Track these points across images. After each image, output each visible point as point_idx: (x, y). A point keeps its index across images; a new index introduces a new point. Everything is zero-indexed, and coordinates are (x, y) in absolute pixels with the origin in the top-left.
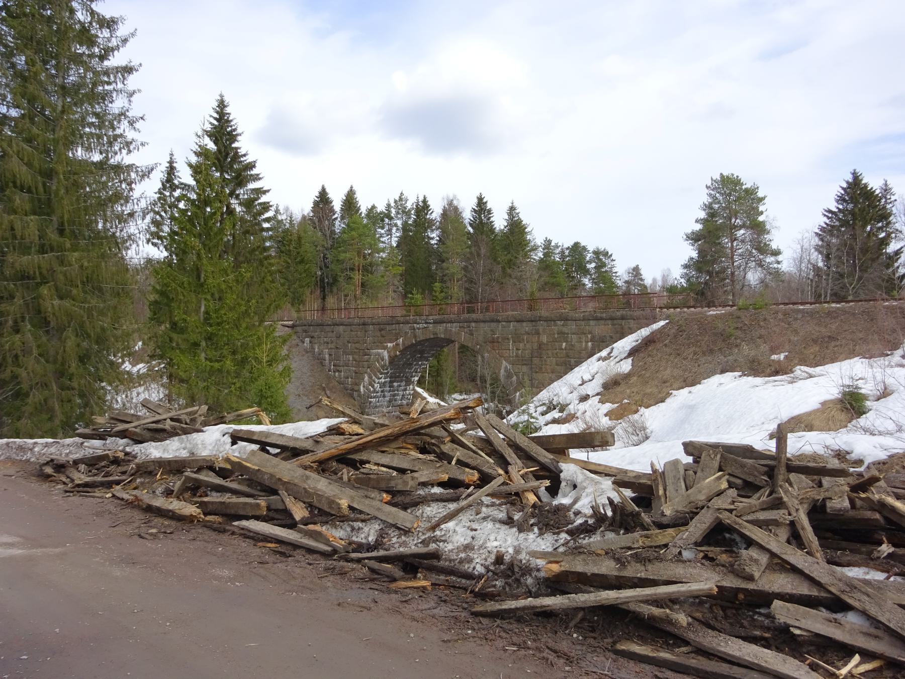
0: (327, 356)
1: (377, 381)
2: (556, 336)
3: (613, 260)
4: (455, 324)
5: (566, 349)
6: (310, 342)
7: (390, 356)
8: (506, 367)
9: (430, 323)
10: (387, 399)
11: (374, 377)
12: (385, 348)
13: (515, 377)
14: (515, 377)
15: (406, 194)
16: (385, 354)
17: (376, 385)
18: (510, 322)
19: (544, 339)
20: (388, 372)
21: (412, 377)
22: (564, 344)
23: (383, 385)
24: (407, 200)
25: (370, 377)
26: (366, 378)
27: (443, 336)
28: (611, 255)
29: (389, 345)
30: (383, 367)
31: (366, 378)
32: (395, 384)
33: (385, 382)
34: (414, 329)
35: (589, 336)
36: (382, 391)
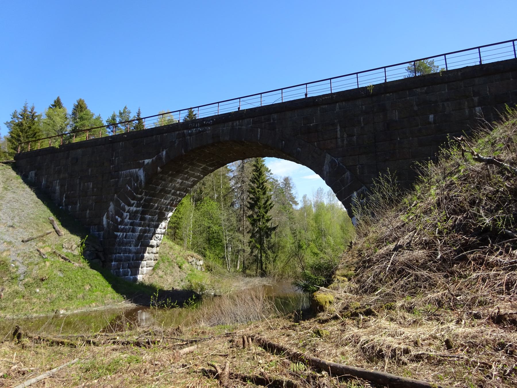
0: (57, 188)
1: (127, 208)
2: (416, 108)
3: (271, 174)
4: (246, 121)
5: (435, 122)
6: (36, 174)
7: (146, 176)
8: (332, 162)
9: (208, 125)
10: (137, 234)
11: (123, 204)
12: (140, 166)
13: (348, 174)
14: (348, 174)
15: (129, 108)
16: (141, 173)
17: (125, 214)
18: (337, 102)
19: (395, 115)
20: (141, 199)
21: (166, 210)
22: (431, 117)
23: (133, 216)
24: (130, 113)
25: (117, 204)
26: (112, 207)
27: (227, 138)
28: (270, 171)
29: (147, 161)
30: (136, 190)
31: (112, 207)
32: (148, 217)
33: (137, 212)
34: (184, 135)
35: (476, 99)
36: (132, 224)
